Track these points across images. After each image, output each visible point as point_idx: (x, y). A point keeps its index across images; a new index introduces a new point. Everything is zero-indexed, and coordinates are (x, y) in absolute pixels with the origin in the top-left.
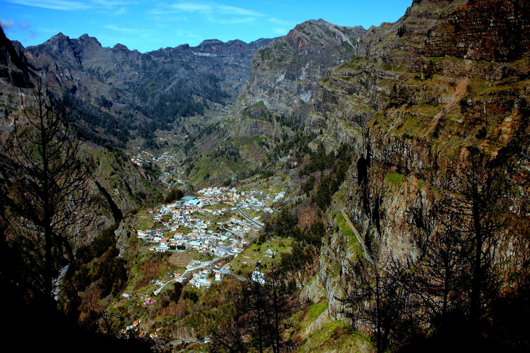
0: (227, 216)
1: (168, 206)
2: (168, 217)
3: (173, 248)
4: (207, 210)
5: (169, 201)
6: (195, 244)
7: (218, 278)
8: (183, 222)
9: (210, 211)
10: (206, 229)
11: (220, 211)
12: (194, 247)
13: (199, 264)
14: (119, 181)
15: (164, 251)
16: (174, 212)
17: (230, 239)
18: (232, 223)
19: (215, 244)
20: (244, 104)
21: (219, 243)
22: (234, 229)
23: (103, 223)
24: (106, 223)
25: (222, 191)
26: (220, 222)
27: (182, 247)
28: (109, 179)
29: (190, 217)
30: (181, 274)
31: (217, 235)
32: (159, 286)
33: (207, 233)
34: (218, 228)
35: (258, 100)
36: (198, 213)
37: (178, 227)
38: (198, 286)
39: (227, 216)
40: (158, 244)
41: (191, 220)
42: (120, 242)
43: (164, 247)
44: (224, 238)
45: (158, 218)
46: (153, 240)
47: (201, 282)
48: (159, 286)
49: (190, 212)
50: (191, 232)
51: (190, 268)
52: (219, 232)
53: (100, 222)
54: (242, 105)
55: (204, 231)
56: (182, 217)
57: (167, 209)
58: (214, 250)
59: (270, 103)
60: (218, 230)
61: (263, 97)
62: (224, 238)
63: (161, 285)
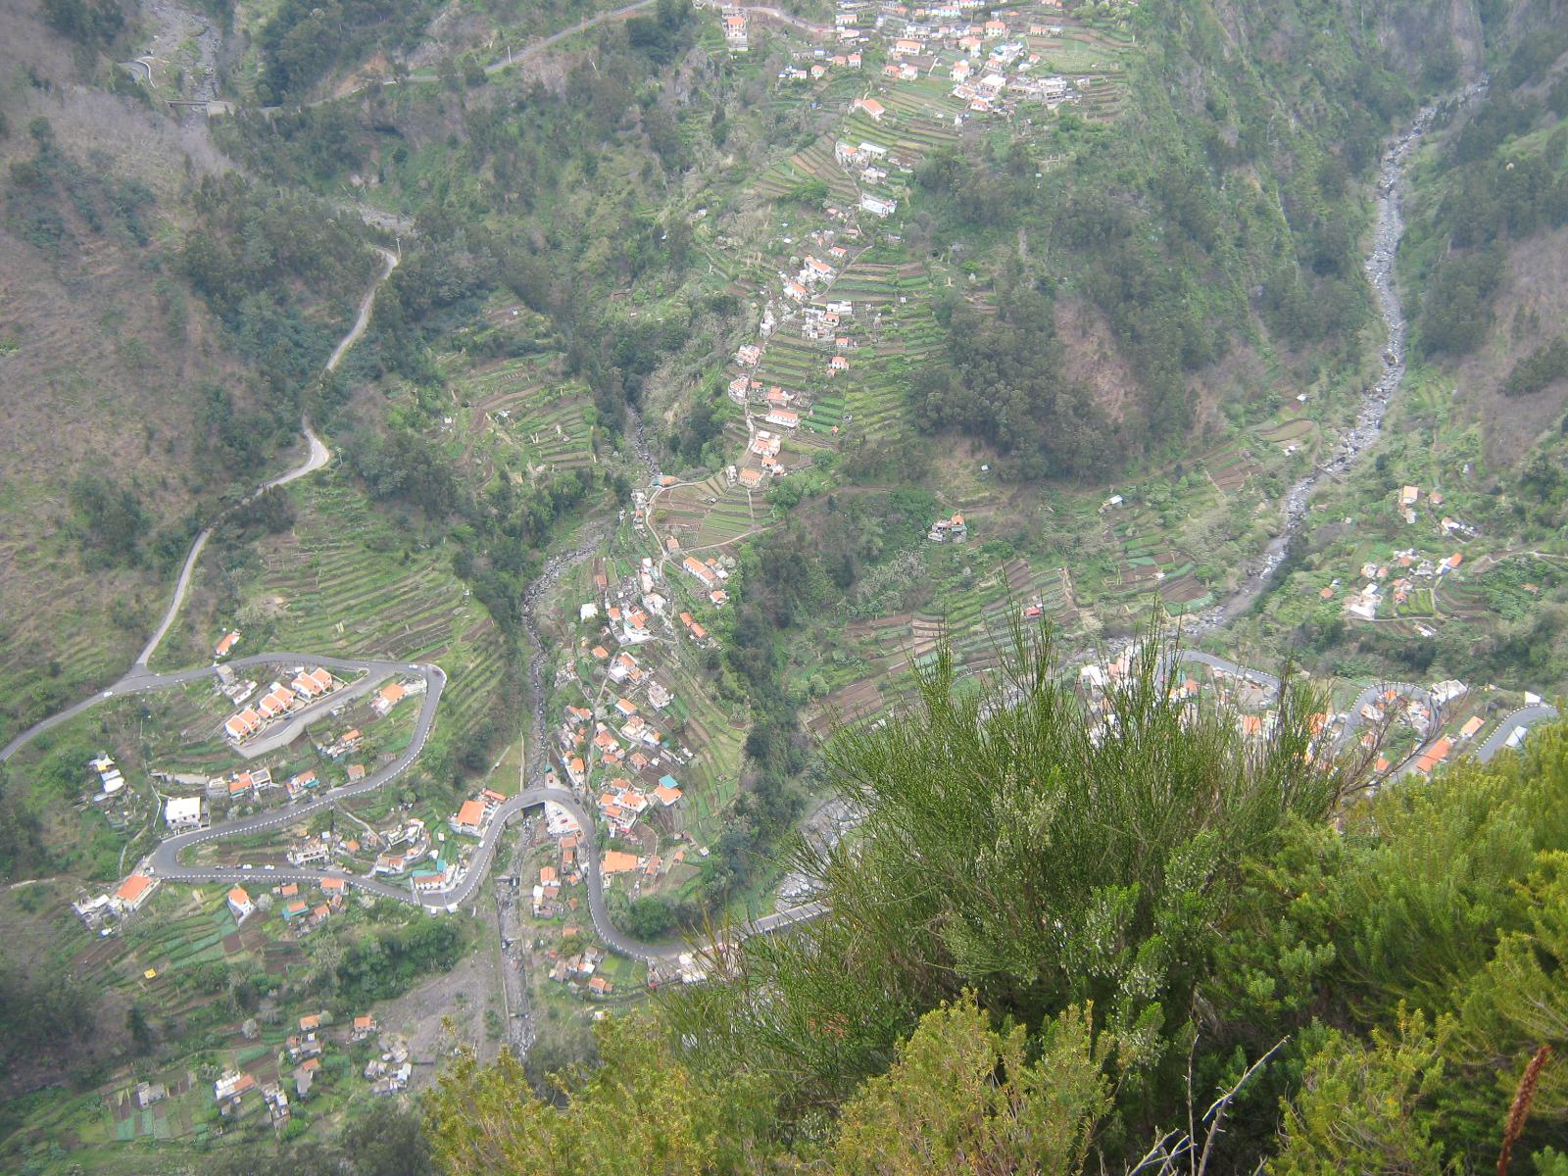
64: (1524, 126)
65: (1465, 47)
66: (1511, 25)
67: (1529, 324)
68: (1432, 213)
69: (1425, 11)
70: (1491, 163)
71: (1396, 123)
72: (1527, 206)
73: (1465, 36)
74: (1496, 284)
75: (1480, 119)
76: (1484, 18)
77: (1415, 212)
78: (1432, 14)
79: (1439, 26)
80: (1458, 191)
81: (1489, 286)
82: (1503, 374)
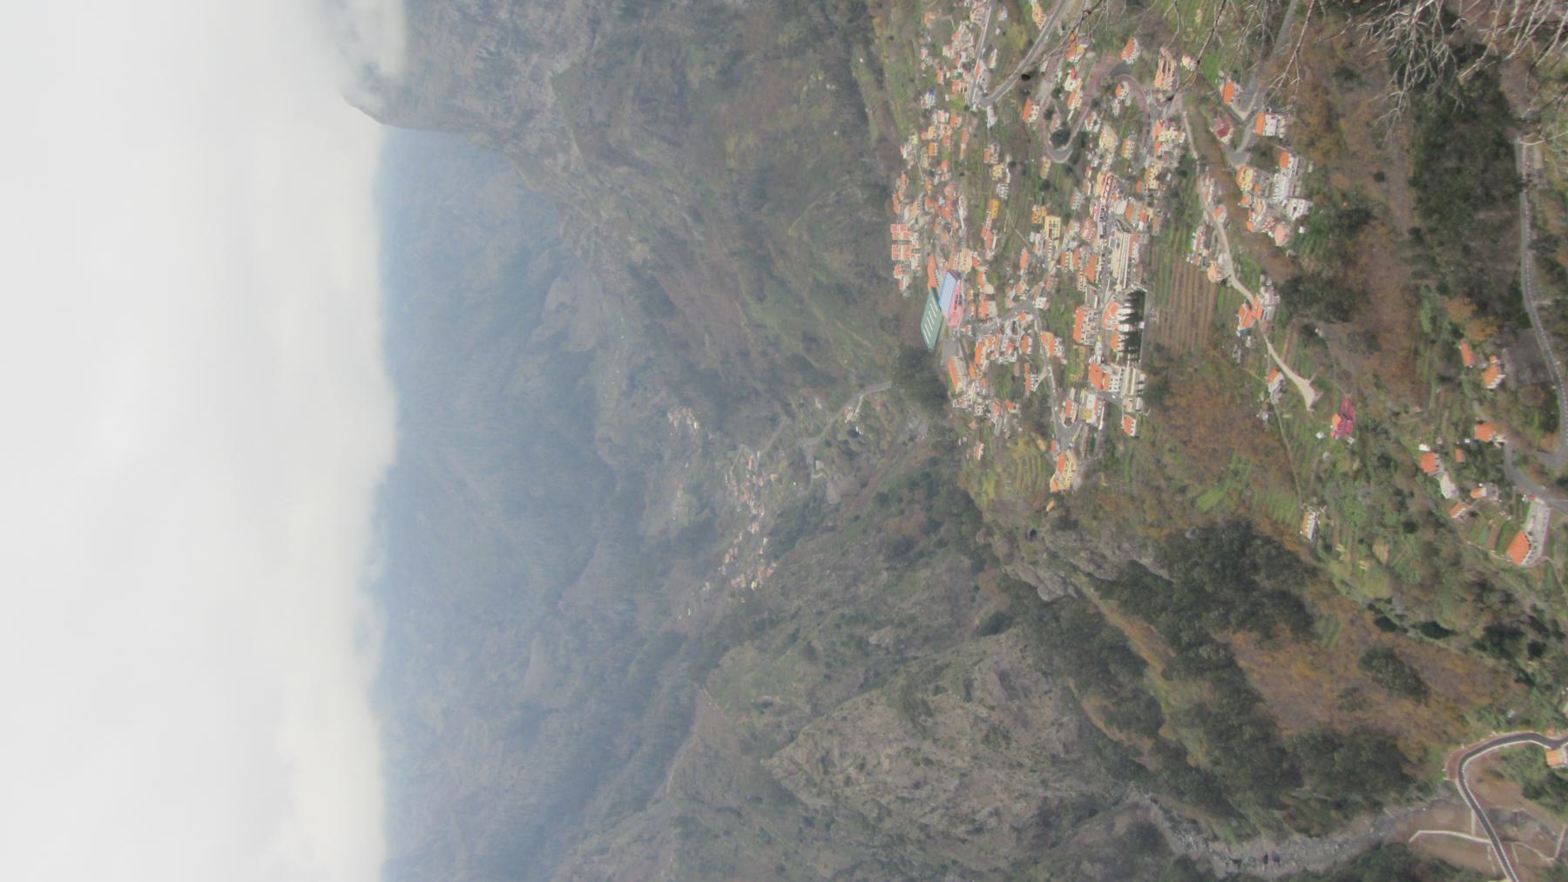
0: (1018, 142)
1: (960, 386)
2: (1003, 379)
3: (1133, 340)
4: (989, 222)
5: (937, 394)
6: (1123, 254)
7: (1271, 126)
8: (1030, 318)
9: (992, 213)
10: (1067, 218)
11: (997, 171)
12: (1135, 254)
13: (1209, 229)
14: (838, 626)
15: (1142, 377)
16: (985, 363)
17: (1117, 111)
18: (1049, 115)
19: (1128, 177)
20: (561, 159)
21: (1127, 153)
22: (1075, 104)
23: (1003, 677)
24: (1005, 665)
25: (911, 198)
26: (1039, 166)
27: (1137, 299)
28: (829, 665)
29: (1012, 294)
30: (1242, 298)
31: (1096, 170)
32: (1286, 388)
33: (1083, 215)
34: (1068, 170)
35: (549, 96)
36: (998, 260)
37: (1049, 335)
38: (1300, 208)
39: (1018, 142)
40: (1111, 409)
41: (1023, 286)
42: (1091, 560)
43: (1126, 382)
44: (1108, 140)
45: (1001, 417)
46: (1093, 429)
47: (1281, 200)
48: (1286, 388)
49: (991, 297)
50: (1073, 278)
51: (1222, 267)
52: (1086, 163)
53: (997, 690)
54: (565, 169)
55: (1075, 227)
56: (1008, 325)
57: (968, 390)
58: (1155, 172)
59: (564, 47)
60: (1075, 169)
61: (535, 77)
62: (1108, 140)
63: (1286, 379)
64: (1177, 754)
65: (1122, 824)
66: (1095, 788)
67: (1353, 698)
68: (1277, 814)
69: (1099, 866)
70: (1218, 770)
71: (1201, 868)
72: (1248, 731)
73: (1113, 825)
74: (1326, 740)
75: (1180, 794)
76: (1093, 813)
77: (1280, 829)
78: (1100, 860)
79: (1109, 851)
80: (1250, 794)
81: (1327, 743)
82: (1408, 705)
